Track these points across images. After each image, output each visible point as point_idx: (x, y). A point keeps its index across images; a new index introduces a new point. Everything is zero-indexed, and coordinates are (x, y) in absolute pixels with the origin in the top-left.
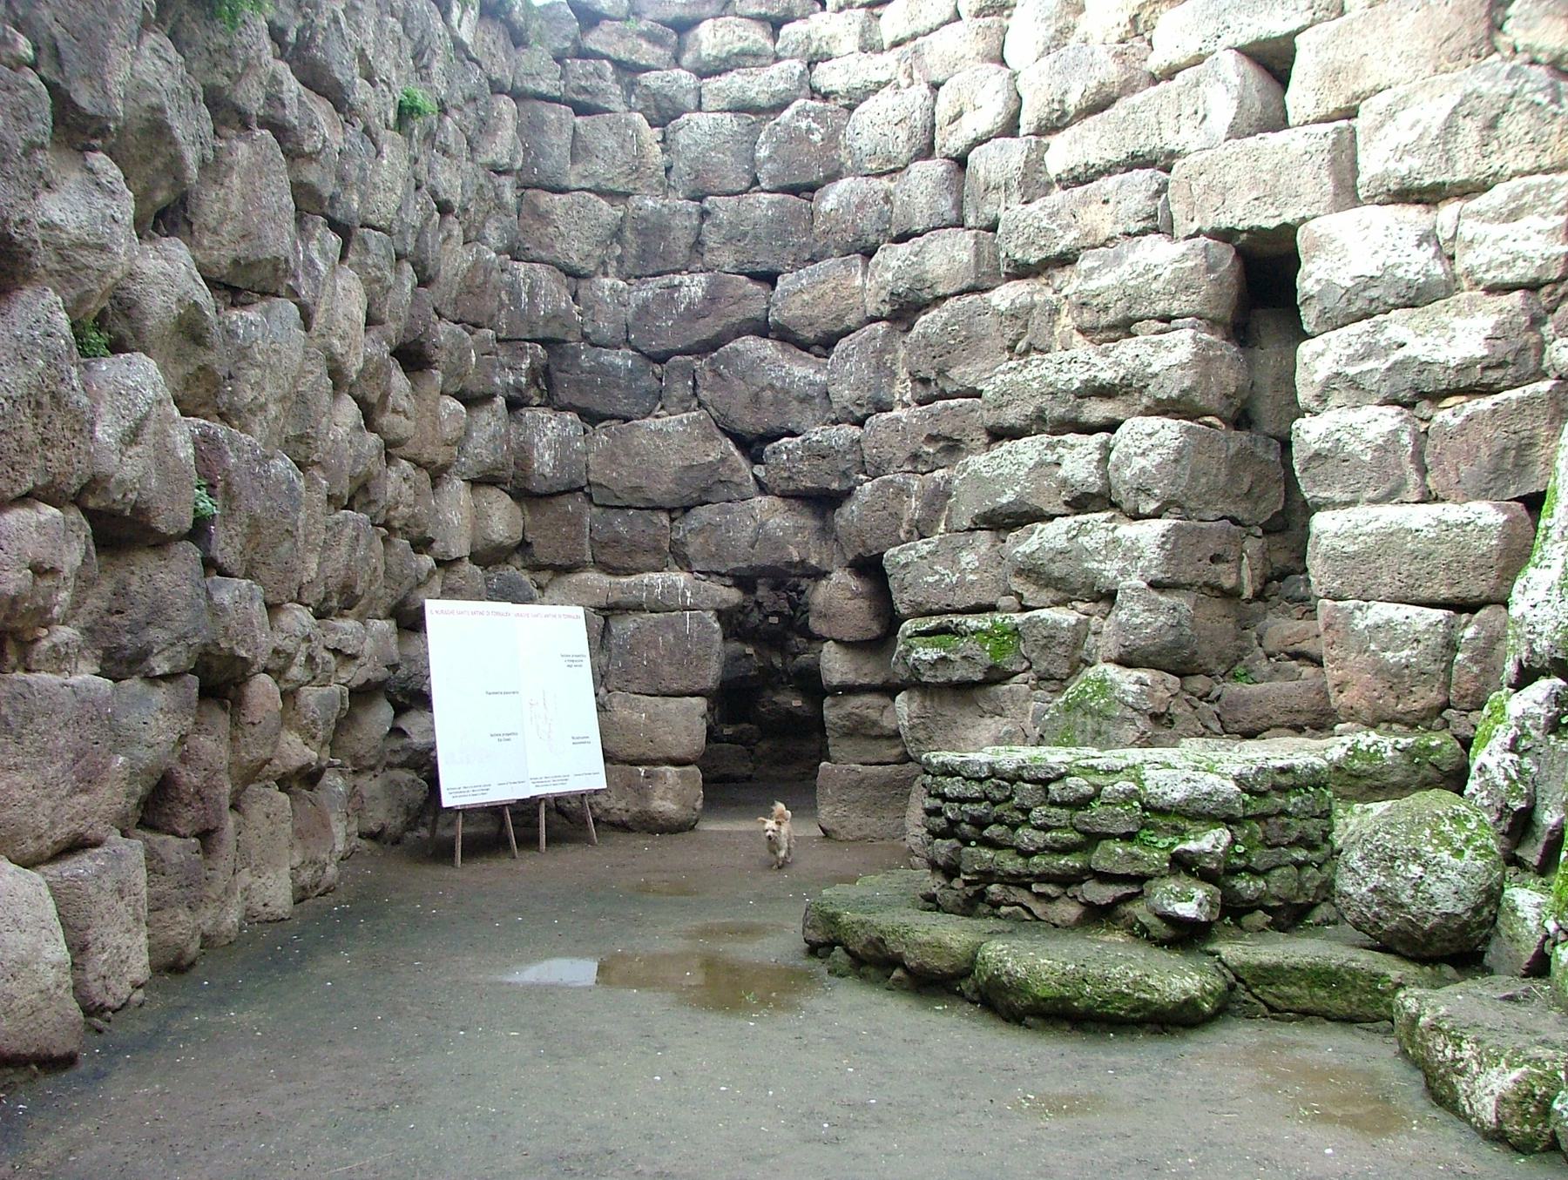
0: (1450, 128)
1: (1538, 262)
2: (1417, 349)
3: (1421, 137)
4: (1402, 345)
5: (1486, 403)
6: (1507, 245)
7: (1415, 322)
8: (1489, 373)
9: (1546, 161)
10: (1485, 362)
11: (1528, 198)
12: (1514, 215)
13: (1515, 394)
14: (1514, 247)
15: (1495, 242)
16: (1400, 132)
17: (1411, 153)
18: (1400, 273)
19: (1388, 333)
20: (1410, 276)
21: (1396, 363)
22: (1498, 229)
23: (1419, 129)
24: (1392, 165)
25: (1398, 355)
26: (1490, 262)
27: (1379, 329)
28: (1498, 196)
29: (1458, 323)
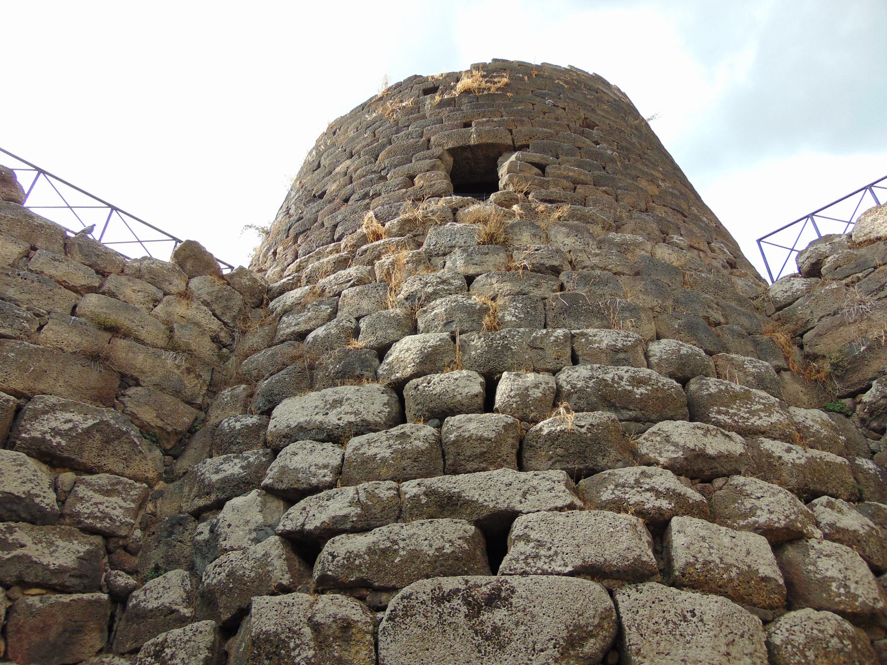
0: (88, 432)
1: (118, 524)
2: (32, 550)
3: (70, 429)
4: (23, 546)
5: (66, 598)
6: (102, 507)
7: (34, 534)
8: (72, 579)
9: (128, 472)
10: (73, 573)
11: (119, 487)
12: (108, 493)
13: (86, 596)
14: (107, 510)
15: (96, 504)
16: (59, 420)
17: (61, 435)
18: (37, 500)
19: (16, 536)
20: (43, 505)
21: (15, 557)
22: (98, 498)
23: (70, 425)
24: (48, 437)
25: (19, 552)
26: (91, 513)
27: (11, 531)
28: (102, 479)
29: (60, 542)
